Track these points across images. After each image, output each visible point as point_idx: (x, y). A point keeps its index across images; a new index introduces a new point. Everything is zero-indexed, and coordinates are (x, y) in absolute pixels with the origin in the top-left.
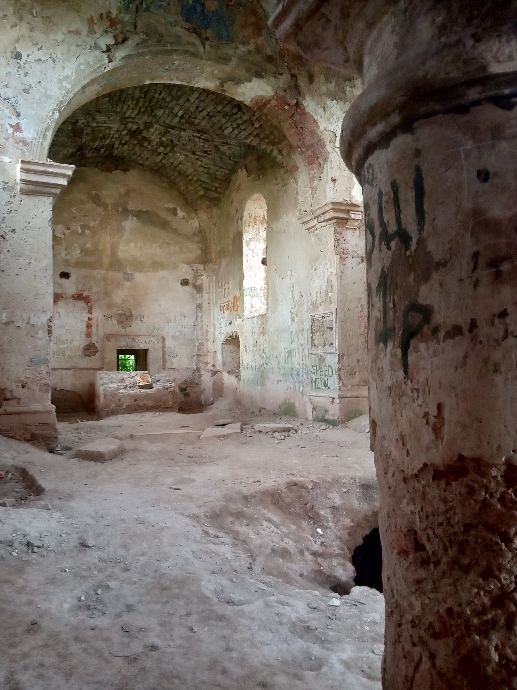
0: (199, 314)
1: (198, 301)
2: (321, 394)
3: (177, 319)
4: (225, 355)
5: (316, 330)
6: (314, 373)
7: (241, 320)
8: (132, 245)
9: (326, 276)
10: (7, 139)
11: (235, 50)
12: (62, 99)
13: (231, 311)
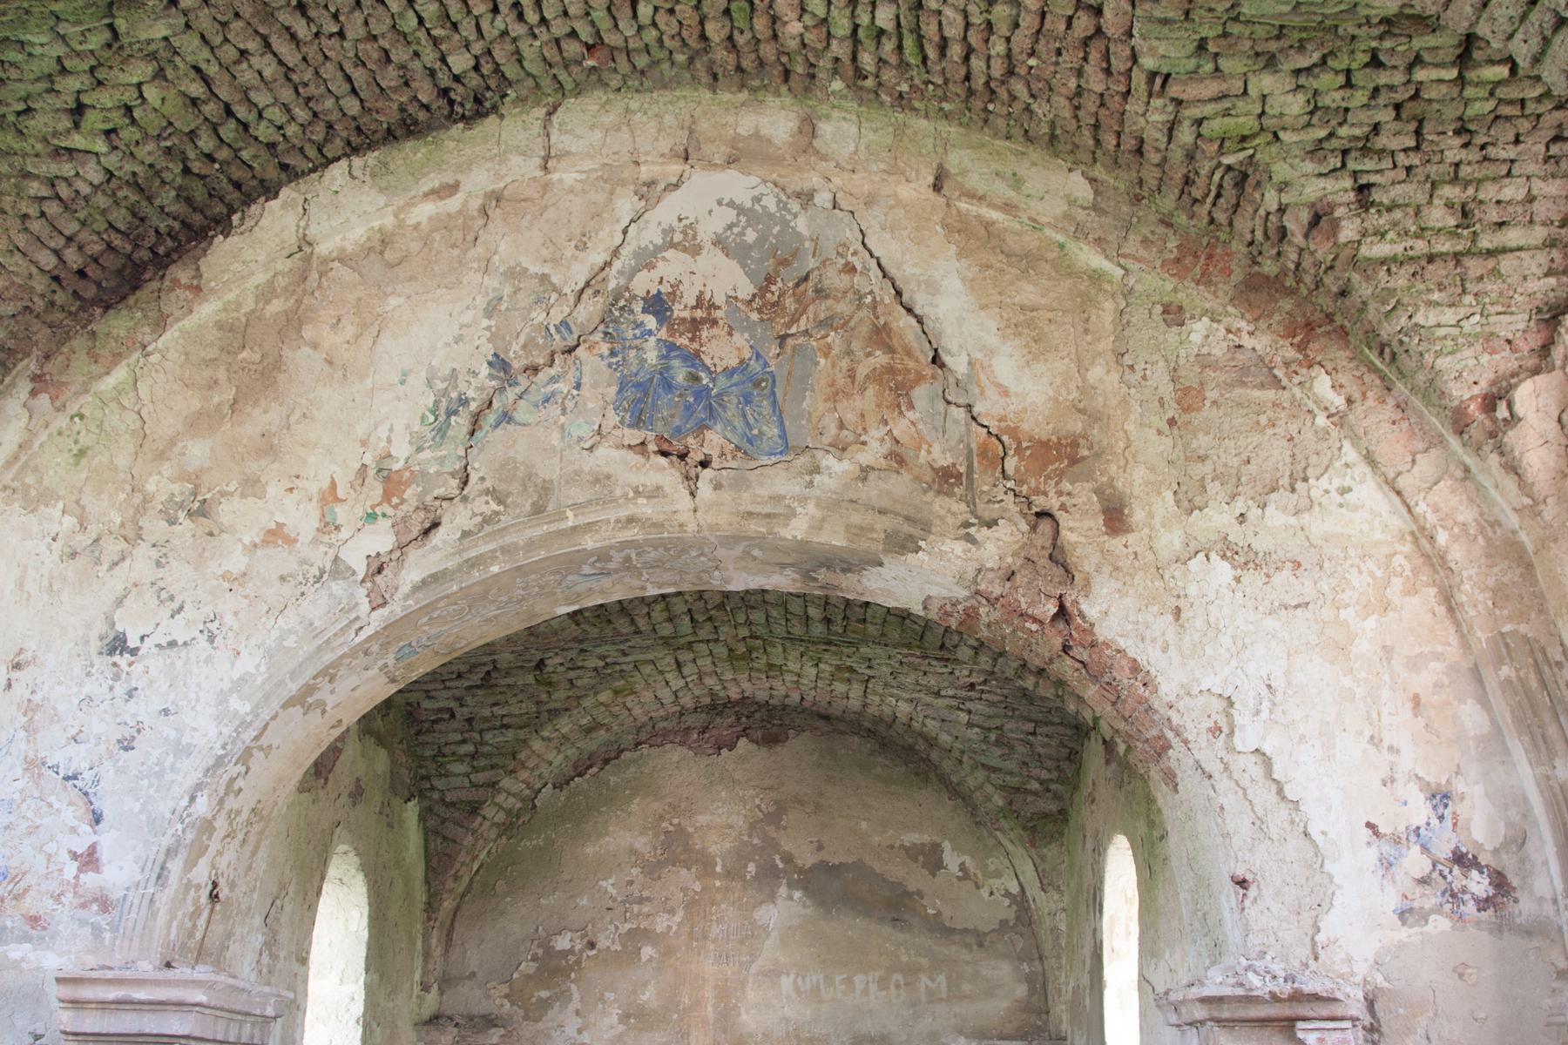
8: (786, 982)
10: (57, 898)
11: (808, 478)
12: (221, 752)
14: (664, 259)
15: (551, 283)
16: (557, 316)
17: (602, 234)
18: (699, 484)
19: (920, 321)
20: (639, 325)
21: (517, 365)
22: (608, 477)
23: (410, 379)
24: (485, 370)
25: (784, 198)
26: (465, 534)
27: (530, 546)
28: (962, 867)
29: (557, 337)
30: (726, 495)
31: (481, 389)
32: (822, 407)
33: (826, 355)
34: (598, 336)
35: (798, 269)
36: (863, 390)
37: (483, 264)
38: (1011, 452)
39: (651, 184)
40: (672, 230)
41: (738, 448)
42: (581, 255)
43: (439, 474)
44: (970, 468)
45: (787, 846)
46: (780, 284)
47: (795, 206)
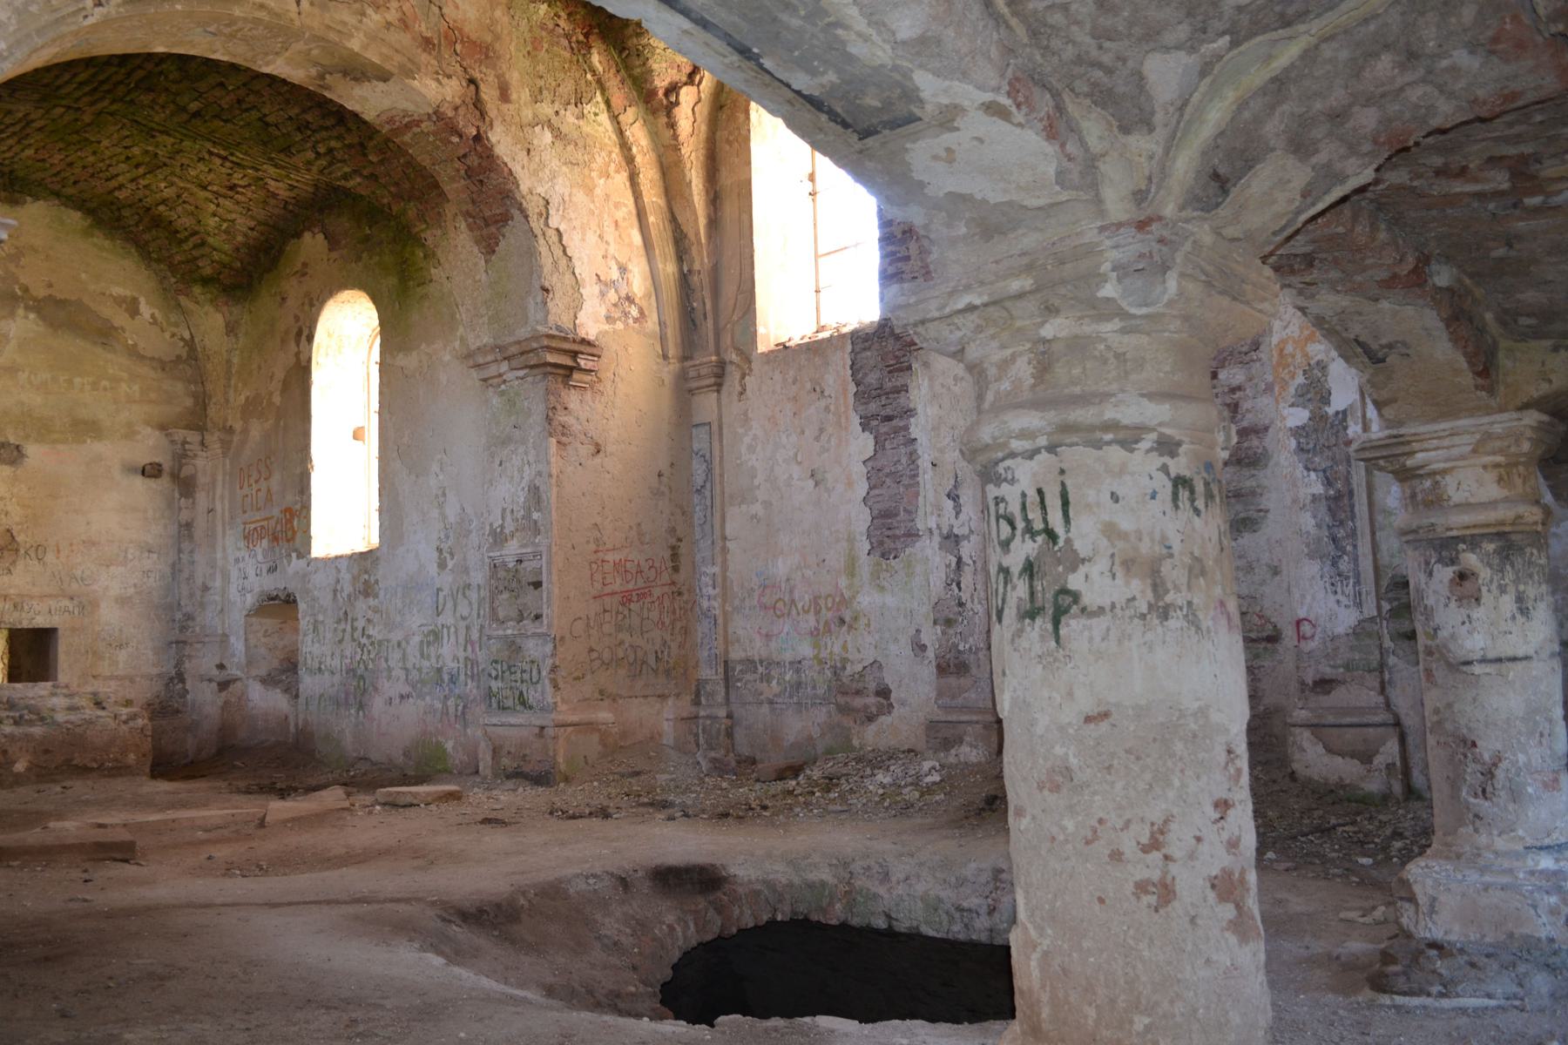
0: (186, 546)
1: (184, 516)
2: (513, 720)
3: (130, 557)
4: (252, 642)
5: (501, 588)
6: (496, 678)
7: (302, 562)
8: (22, 376)
9: (527, 478)
13: (275, 539)
28: (153, 316)
45: (23, 280)
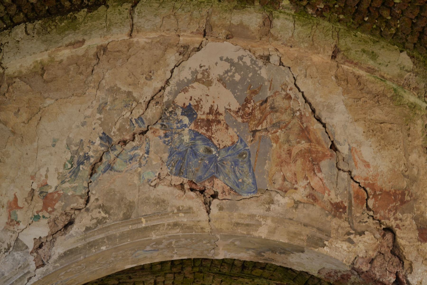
14: (192, 87)
15: (133, 96)
16: (137, 113)
17: (160, 72)
18: (211, 207)
19: (324, 126)
20: (180, 121)
21: (115, 140)
22: (164, 201)
23: (58, 144)
24: (98, 141)
25: (255, 59)
26: (88, 229)
27: (123, 236)
29: (136, 125)
30: (225, 213)
31: (96, 151)
32: (274, 169)
33: (277, 142)
34: (158, 126)
35: (261, 97)
36: (295, 161)
37: (97, 85)
38: (371, 197)
39: (186, 47)
40: (196, 72)
41: (231, 189)
42: (148, 82)
43: (73, 196)
44: (350, 203)
46: (253, 104)
47: (260, 63)
